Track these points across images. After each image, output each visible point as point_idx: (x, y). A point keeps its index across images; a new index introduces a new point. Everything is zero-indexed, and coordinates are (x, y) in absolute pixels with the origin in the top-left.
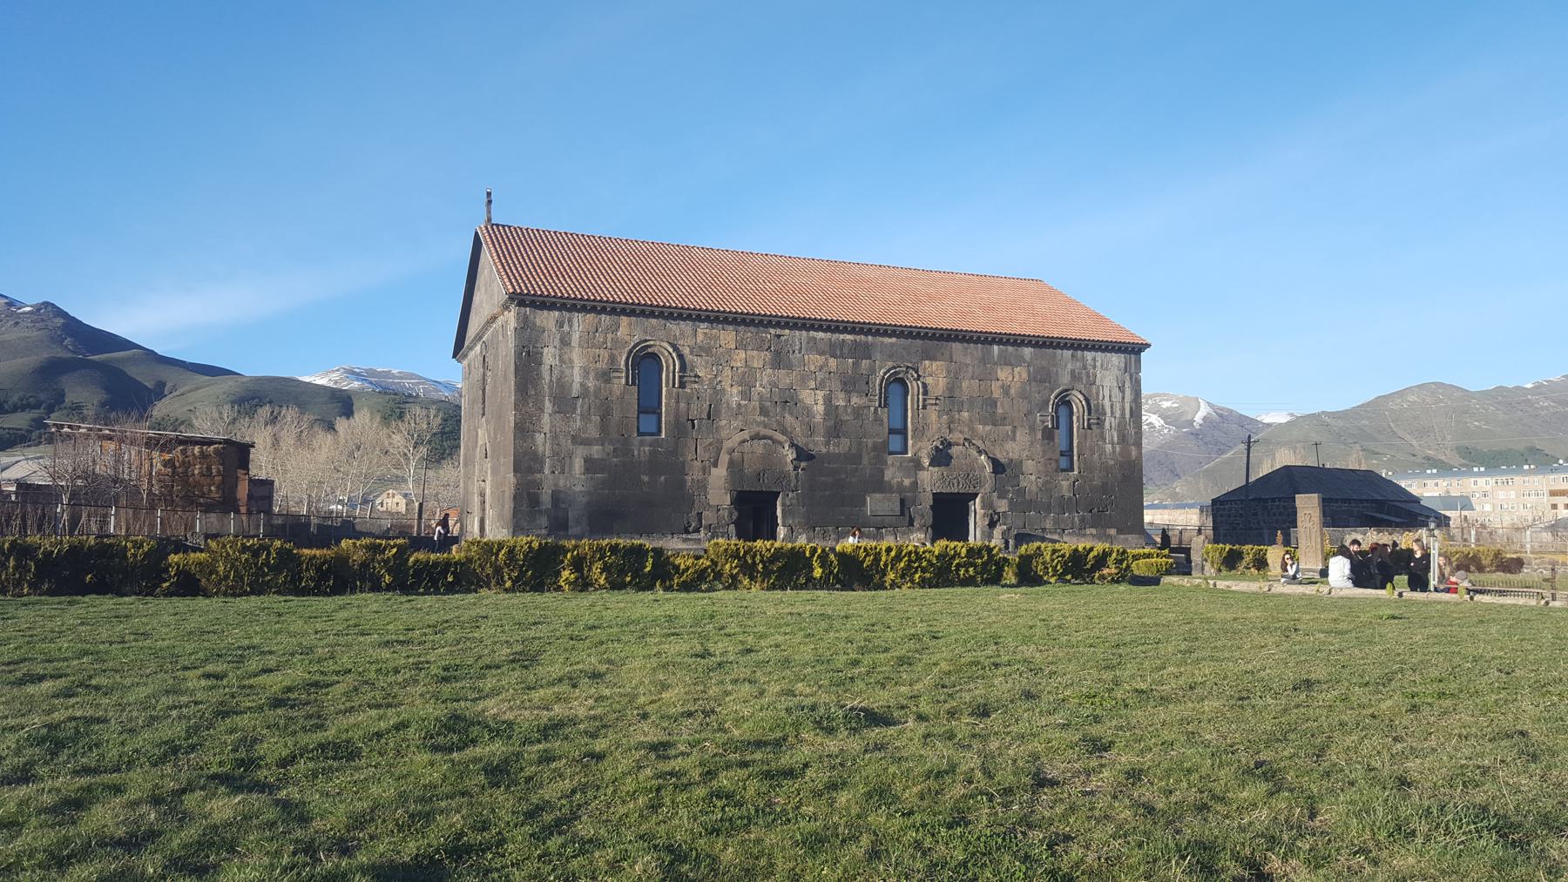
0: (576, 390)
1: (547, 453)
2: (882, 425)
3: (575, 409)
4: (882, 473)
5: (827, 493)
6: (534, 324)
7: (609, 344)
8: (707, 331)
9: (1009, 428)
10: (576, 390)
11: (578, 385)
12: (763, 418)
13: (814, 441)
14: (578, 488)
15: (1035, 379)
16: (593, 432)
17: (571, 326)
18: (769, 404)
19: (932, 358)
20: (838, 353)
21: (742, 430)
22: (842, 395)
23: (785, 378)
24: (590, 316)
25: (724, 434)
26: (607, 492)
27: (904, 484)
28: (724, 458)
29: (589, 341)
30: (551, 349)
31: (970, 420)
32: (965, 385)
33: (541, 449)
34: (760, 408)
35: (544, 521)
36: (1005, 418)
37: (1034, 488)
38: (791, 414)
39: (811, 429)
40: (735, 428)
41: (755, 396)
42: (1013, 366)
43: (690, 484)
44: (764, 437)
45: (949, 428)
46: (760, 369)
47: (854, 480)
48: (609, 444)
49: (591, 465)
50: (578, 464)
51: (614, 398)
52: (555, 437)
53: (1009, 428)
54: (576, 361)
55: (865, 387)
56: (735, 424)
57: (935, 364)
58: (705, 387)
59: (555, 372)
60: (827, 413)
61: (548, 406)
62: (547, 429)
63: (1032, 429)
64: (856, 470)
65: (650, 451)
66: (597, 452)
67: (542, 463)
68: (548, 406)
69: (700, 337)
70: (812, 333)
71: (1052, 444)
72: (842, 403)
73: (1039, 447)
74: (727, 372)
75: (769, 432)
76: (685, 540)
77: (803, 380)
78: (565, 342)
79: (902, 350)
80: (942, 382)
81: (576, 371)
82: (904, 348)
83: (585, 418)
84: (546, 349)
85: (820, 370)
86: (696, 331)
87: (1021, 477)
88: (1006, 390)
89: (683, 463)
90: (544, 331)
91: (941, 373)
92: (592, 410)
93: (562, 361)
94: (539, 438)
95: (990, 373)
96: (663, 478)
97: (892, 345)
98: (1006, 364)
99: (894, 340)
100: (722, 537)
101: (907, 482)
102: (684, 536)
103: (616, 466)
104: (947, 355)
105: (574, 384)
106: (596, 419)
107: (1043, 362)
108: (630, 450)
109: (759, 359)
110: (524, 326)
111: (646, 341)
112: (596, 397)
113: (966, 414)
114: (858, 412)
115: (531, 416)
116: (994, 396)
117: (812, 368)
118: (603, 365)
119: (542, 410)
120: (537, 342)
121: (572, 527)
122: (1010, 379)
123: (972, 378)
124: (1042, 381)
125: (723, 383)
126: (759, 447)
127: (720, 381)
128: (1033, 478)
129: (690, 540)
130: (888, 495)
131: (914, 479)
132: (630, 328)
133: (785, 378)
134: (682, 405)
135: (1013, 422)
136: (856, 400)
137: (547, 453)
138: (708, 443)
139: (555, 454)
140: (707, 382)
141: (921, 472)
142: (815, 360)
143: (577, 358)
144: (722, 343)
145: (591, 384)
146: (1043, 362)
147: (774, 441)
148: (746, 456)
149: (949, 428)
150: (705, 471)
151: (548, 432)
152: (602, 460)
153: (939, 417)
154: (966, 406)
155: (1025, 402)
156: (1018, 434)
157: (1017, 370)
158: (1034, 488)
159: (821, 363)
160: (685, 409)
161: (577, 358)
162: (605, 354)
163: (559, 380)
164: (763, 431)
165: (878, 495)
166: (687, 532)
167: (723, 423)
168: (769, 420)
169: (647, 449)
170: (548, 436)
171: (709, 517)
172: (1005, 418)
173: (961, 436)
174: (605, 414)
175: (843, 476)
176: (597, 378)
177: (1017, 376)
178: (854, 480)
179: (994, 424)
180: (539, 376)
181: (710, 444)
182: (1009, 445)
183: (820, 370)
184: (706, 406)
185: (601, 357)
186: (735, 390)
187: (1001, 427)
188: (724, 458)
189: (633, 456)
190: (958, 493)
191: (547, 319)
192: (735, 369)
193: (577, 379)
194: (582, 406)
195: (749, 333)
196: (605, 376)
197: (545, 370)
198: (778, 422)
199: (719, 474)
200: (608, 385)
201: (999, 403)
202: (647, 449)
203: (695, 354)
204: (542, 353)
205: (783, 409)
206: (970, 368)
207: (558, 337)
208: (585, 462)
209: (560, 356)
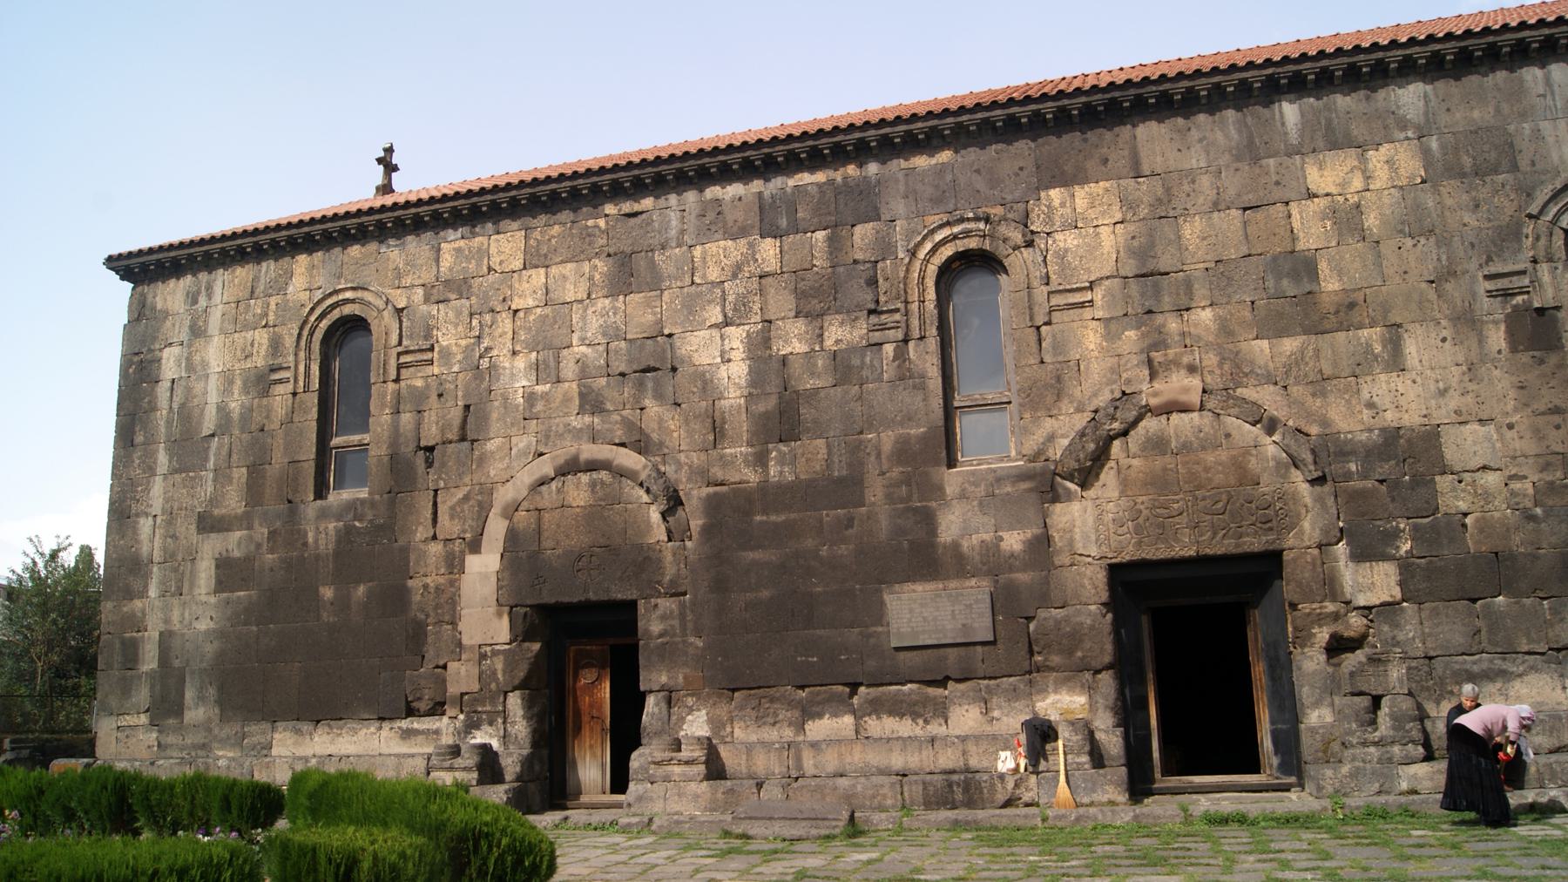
0: (208, 426)
1: (157, 557)
2: (922, 387)
3: (206, 459)
4: (928, 520)
5: (765, 594)
6: (154, 308)
7: (271, 317)
8: (462, 243)
9: (1372, 336)
10: (208, 426)
11: (214, 411)
12: (587, 419)
13: (722, 457)
14: (203, 625)
15: (1454, 171)
16: (234, 502)
17: (209, 297)
18: (603, 381)
19: (1068, 179)
20: (784, 223)
21: (541, 454)
22: (800, 326)
23: (638, 312)
24: (242, 273)
25: (494, 470)
26: (254, 628)
27: (1003, 545)
28: (496, 528)
29: (237, 322)
30: (176, 350)
31: (1226, 330)
32: (1191, 231)
33: (145, 550)
34: (581, 395)
35: (143, 695)
36: (1352, 305)
37: (1500, 510)
38: (659, 396)
39: (717, 430)
40: (524, 453)
41: (569, 369)
42: (1361, 147)
43: (418, 598)
44: (593, 466)
45: (1150, 362)
46: (581, 301)
47: (843, 550)
48: (261, 525)
49: (229, 573)
50: (205, 572)
51: (276, 425)
52: (170, 522)
53: (1372, 336)
54: (213, 363)
55: (867, 297)
56: (522, 442)
57: (1081, 194)
58: (456, 368)
59: (179, 391)
60: (757, 379)
61: (162, 459)
62: (157, 504)
63: (1467, 321)
64: (850, 522)
65: (338, 531)
66: (239, 544)
67: (147, 576)
68: (162, 459)
69: (447, 260)
70: (713, 192)
71: (1553, 359)
72: (799, 347)
73: (1501, 382)
74: (505, 323)
75: (602, 452)
76: (408, 734)
77: (691, 307)
78: (198, 331)
79: (975, 177)
80: (1109, 241)
81: (213, 385)
82: (978, 171)
83: (221, 475)
84: (166, 352)
85: (735, 276)
86: (439, 250)
87: (1443, 482)
88: (1347, 220)
89: (405, 551)
90: (166, 318)
91: (1103, 213)
92: (235, 457)
93: (190, 367)
94: (145, 525)
95: (1277, 183)
96: (361, 590)
97: (941, 169)
98: (1334, 145)
99: (945, 156)
100: (491, 724)
101: (1013, 541)
102: (404, 724)
103: (272, 570)
104: (1119, 159)
105: (207, 412)
106: (240, 474)
107: (1476, 114)
108: (299, 531)
109: (571, 280)
110: (140, 314)
111: (336, 292)
112: (243, 432)
113: (1205, 316)
114: (843, 366)
115: (133, 483)
116: (1300, 246)
117: (714, 274)
118: (260, 361)
119: (151, 471)
120: (155, 339)
121: (190, 709)
122: (1358, 183)
123: (1216, 207)
124: (1481, 172)
125: (495, 352)
126: (578, 492)
127: (488, 349)
128: (1491, 479)
129: (416, 732)
130: (953, 584)
131: (1038, 531)
132: (311, 276)
133: (638, 312)
134: (407, 418)
135: (1386, 309)
136: (838, 333)
137: (157, 557)
138: (460, 495)
139: (169, 557)
140: (459, 357)
141: (1058, 507)
142: (718, 255)
143: (216, 355)
144: (495, 261)
145: (234, 407)
146: (1476, 114)
147: (622, 473)
148: (546, 516)
149: (1150, 362)
150: (455, 565)
151: (159, 512)
152: (248, 560)
153: (1110, 336)
154: (1201, 292)
155: (1427, 245)
156: (1412, 348)
157: (1376, 158)
158: (1500, 510)
159: (736, 256)
160: (410, 427)
161: (216, 355)
162: (262, 337)
163: (182, 406)
164: (589, 451)
165: (919, 587)
166: (410, 712)
167: (491, 446)
168: (603, 422)
169: (331, 526)
170: (159, 520)
171: (462, 677)
172: (1352, 305)
173: (1195, 382)
174: (256, 471)
175: (809, 543)
176: (245, 390)
177: (1381, 177)
178: (843, 550)
179: (1316, 329)
180: (153, 408)
181: (466, 498)
182: (1380, 386)
183: (735, 276)
184: (455, 414)
185: (256, 345)
186: (521, 363)
187: (1341, 336)
188: (496, 528)
189: (305, 544)
190: (1201, 560)
191: (171, 295)
192: (521, 314)
193: (213, 398)
194: (217, 454)
195: (553, 229)
196: (262, 382)
197: (163, 390)
198: (628, 425)
199: (484, 566)
200: (265, 401)
201: (1323, 266)
202: (331, 526)
203: (434, 298)
204: (159, 360)
205: (641, 385)
206: (1205, 181)
207: (188, 323)
208: (217, 567)
209: (188, 359)
